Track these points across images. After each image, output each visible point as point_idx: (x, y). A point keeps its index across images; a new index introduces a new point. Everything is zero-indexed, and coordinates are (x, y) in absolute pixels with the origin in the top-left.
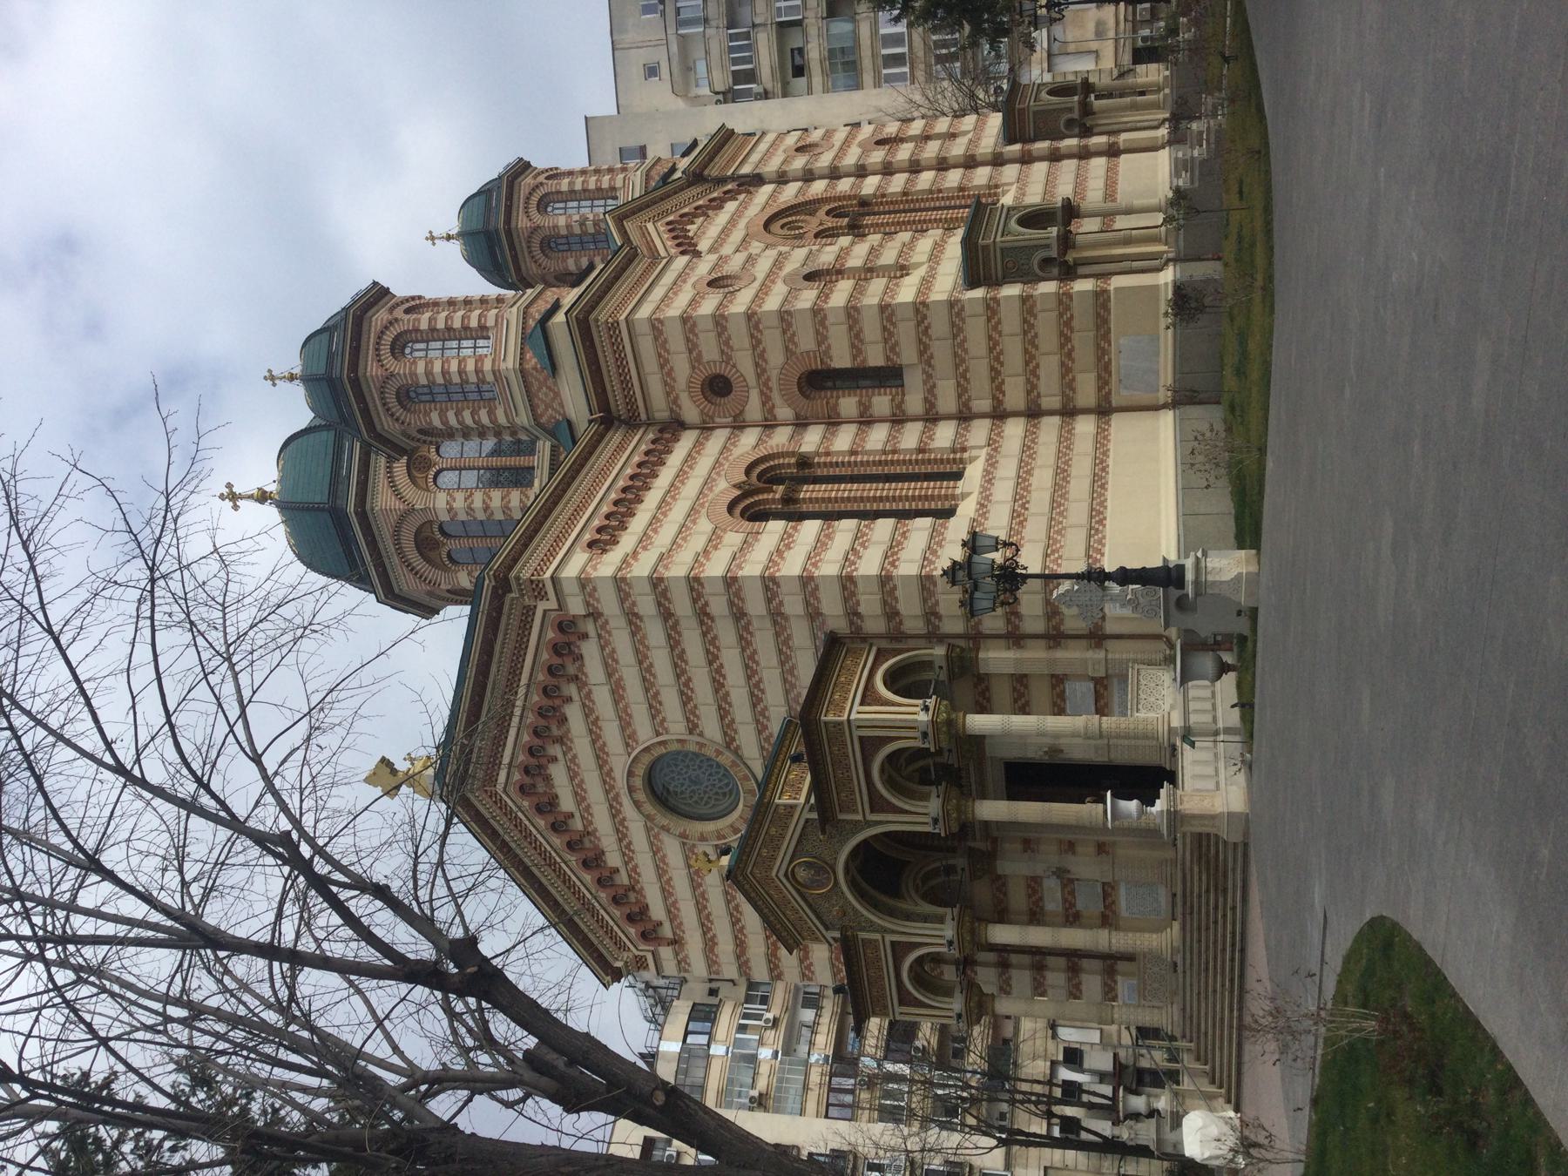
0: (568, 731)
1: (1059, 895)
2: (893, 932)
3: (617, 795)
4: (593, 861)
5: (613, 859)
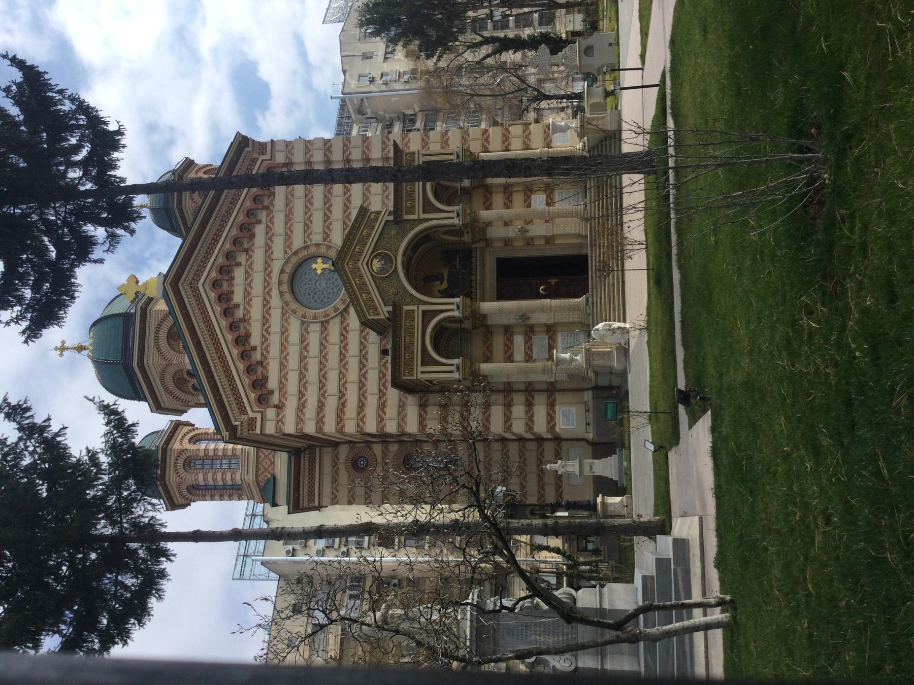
1: (523, 347)
3: (271, 290)
4: (242, 340)
5: (255, 340)
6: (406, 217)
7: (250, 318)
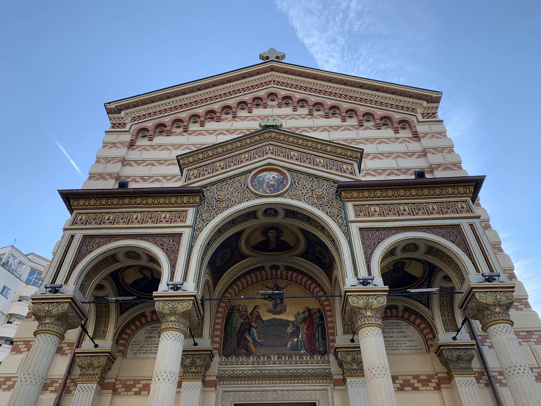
0: (316, 118)
2: (193, 238)
6: (350, 206)
7: (236, 121)
